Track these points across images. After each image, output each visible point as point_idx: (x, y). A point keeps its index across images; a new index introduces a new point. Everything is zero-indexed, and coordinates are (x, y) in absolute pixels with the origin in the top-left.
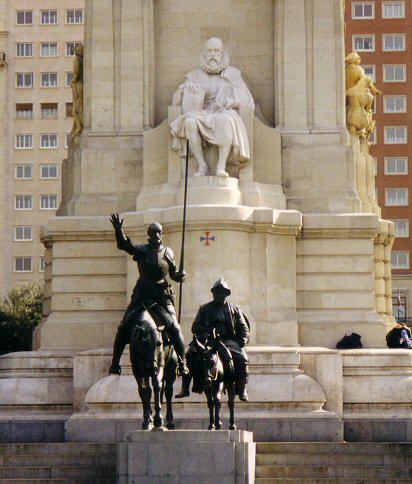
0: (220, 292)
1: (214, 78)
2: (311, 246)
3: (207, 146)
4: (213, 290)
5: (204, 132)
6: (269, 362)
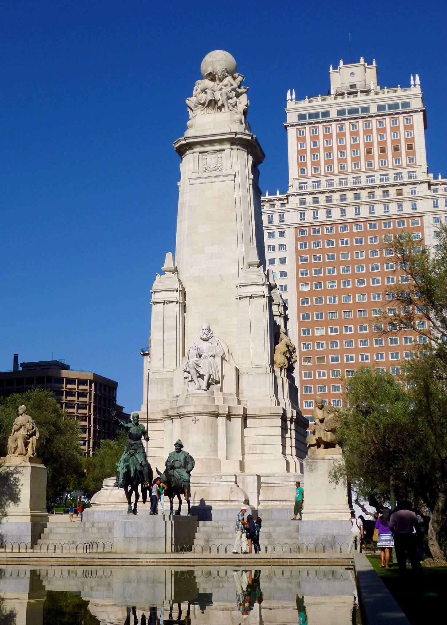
0: (179, 446)
1: (206, 343)
3: (201, 376)
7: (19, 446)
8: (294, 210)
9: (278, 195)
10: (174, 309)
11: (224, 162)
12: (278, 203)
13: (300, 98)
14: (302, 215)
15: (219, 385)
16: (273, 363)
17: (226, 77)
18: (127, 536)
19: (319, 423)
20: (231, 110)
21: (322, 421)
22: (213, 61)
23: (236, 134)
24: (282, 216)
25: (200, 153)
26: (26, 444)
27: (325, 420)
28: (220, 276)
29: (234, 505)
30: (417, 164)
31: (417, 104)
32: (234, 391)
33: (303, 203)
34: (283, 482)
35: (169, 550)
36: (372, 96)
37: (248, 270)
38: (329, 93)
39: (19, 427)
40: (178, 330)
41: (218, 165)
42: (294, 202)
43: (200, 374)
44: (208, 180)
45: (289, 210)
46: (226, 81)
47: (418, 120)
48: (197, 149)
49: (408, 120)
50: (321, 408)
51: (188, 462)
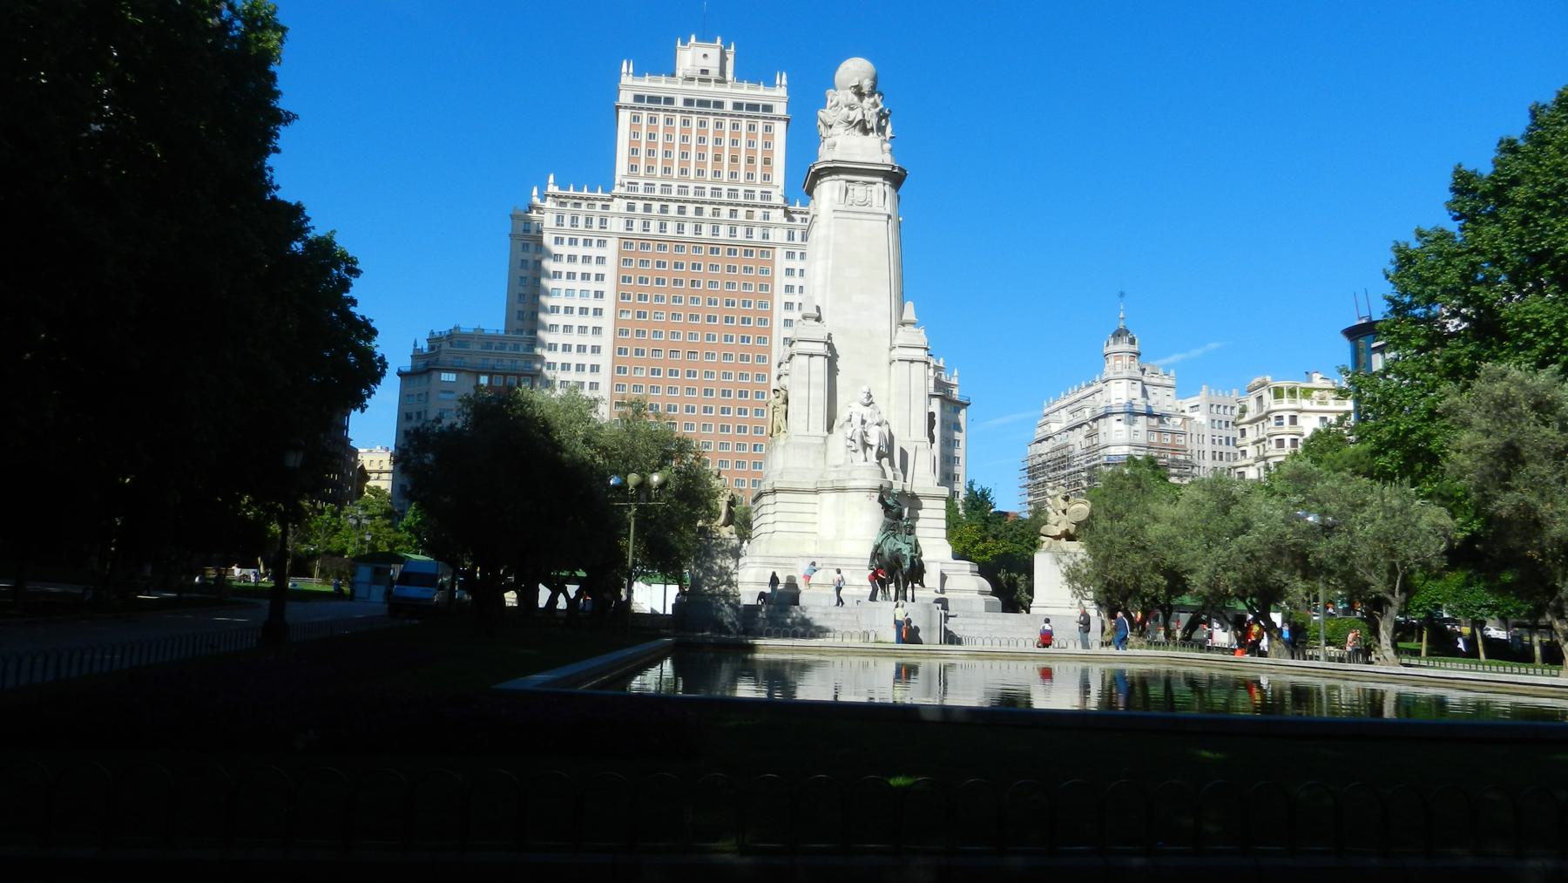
8: (620, 215)
9: (599, 193)
10: (820, 364)
12: (599, 204)
13: (638, 73)
14: (629, 224)
24: (603, 221)
31: (780, 109)
33: (631, 208)
36: (727, 89)
38: (674, 75)
42: (619, 206)
45: (613, 215)
47: (780, 128)
49: (768, 128)
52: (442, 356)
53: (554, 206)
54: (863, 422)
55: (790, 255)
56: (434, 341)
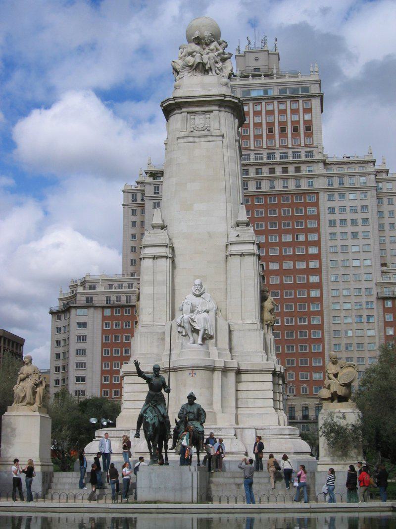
0: (192, 398)
1: (198, 298)
2: (244, 377)
4: (188, 397)
5: (192, 323)
6: (220, 433)
7: (27, 395)
10: (164, 264)
11: (212, 123)
15: (214, 340)
16: (262, 320)
17: (213, 42)
18: (153, 486)
19: (334, 378)
20: (217, 74)
21: (336, 375)
22: (199, 26)
23: (225, 96)
25: (188, 113)
26: (34, 393)
27: (339, 375)
28: (209, 233)
29: (235, 457)
30: (314, 145)
32: (227, 347)
34: (277, 435)
35: (195, 500)
37: (237, 228)
39: (25, 376)
40: (168, 285)
41: (206, 125)
43: (194, 329)
44: (197, 139)
46: (212, 46)
48: (184, 110)
50: (335, 363)
51: (201, 414)
52: (78, 297)
53: (151, 179)
54: (193, 311)
55: (331, 197)
56: (74, 287)
